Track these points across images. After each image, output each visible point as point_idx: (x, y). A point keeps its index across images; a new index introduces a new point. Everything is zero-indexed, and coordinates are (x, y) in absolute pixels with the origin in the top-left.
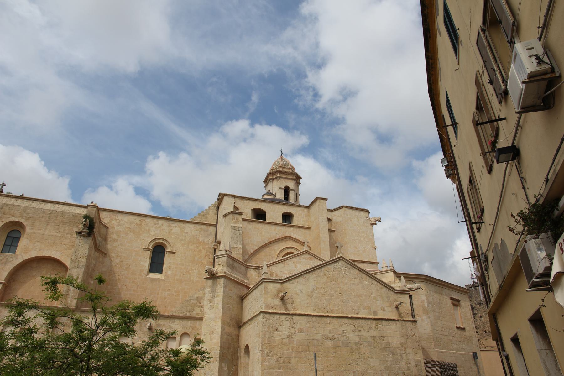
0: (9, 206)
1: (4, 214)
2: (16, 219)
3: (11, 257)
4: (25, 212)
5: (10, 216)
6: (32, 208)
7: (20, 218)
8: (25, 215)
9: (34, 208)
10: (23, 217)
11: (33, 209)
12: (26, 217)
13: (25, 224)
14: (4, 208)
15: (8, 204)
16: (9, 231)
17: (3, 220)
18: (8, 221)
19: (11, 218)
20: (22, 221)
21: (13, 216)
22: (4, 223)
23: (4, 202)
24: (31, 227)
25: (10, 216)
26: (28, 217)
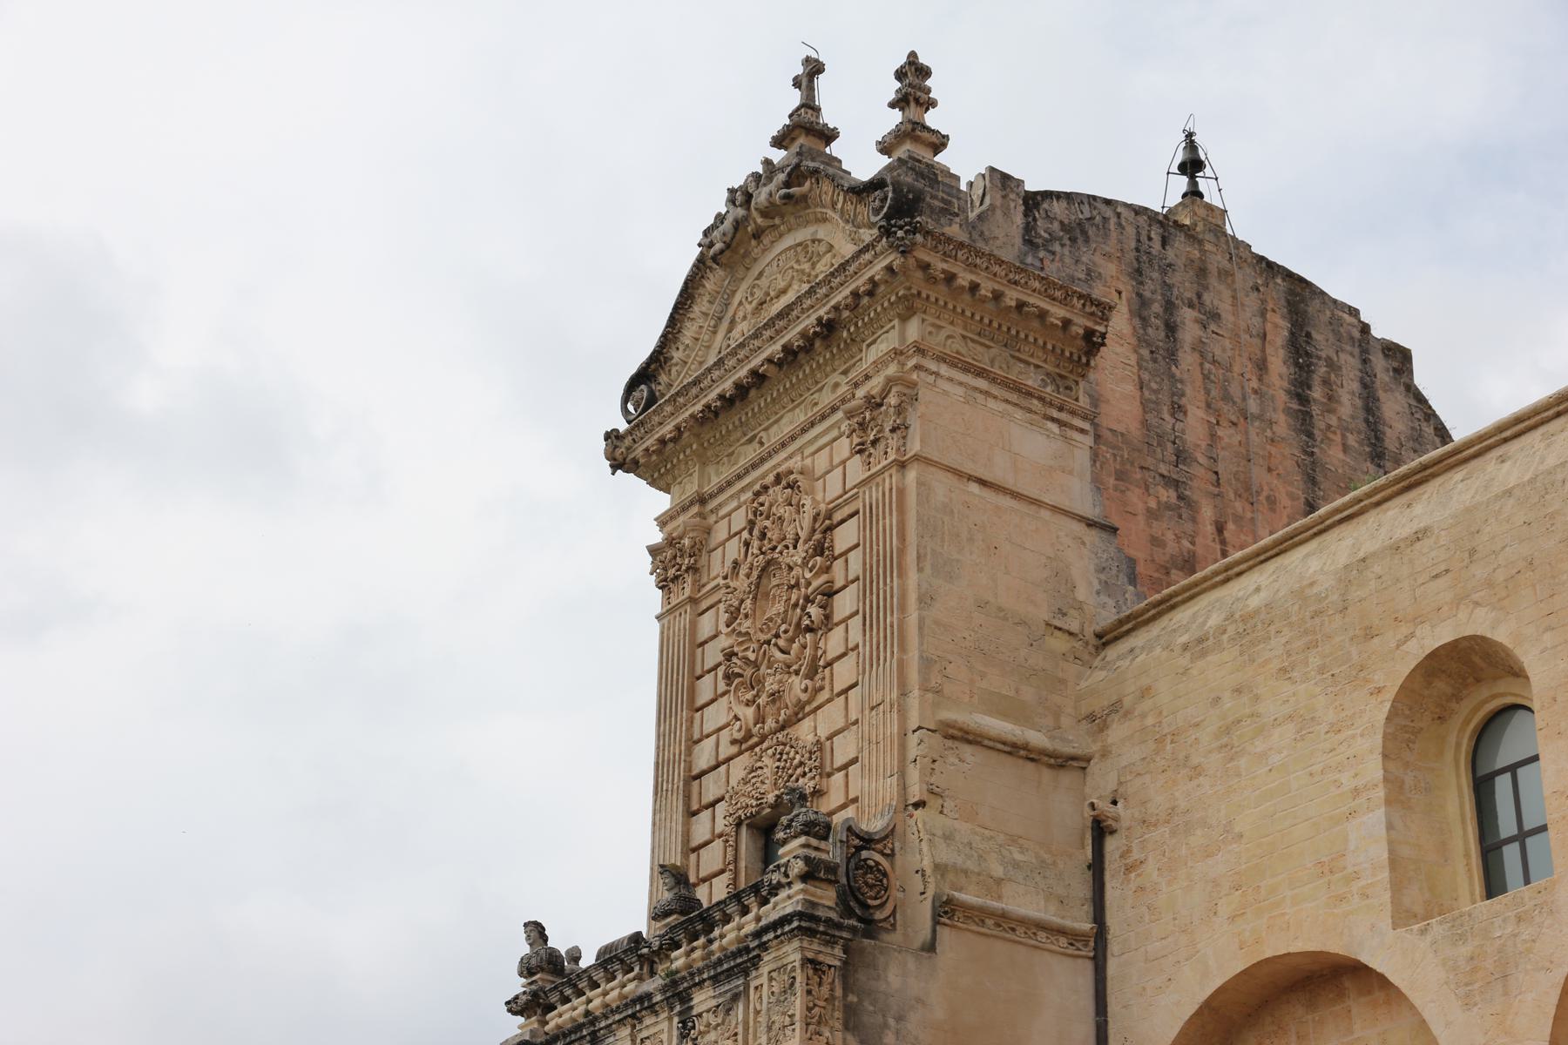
0: (1377, 569)
1: (1369, 634)
2: (1444, 634)
3: (1519, 919)
4: (1472, 552)
5: (1404, 630)
6: (1497, 497)
7: (1462, 615)
8: (1479, 571)
9: (1509, 493)
10: (1475, 597)
11: (1511, 501)
12: (1490, 584)
13: (1501, 636)
14: (1355, 594)
15: (1364, 560)
16: (1466, 745)
17: (1379, 678)
18: (1405, 668)
19: (1412, 645)
20: (1478, 623)
21: (1418, 620)
22: (1389, 695)
23: (1342, 560)
24: (1547, 637)
25: (1404, 630)
26: (1500, 576)
